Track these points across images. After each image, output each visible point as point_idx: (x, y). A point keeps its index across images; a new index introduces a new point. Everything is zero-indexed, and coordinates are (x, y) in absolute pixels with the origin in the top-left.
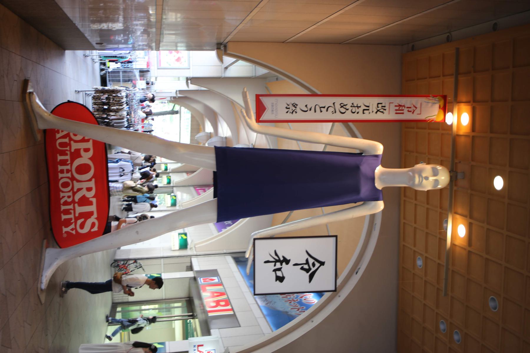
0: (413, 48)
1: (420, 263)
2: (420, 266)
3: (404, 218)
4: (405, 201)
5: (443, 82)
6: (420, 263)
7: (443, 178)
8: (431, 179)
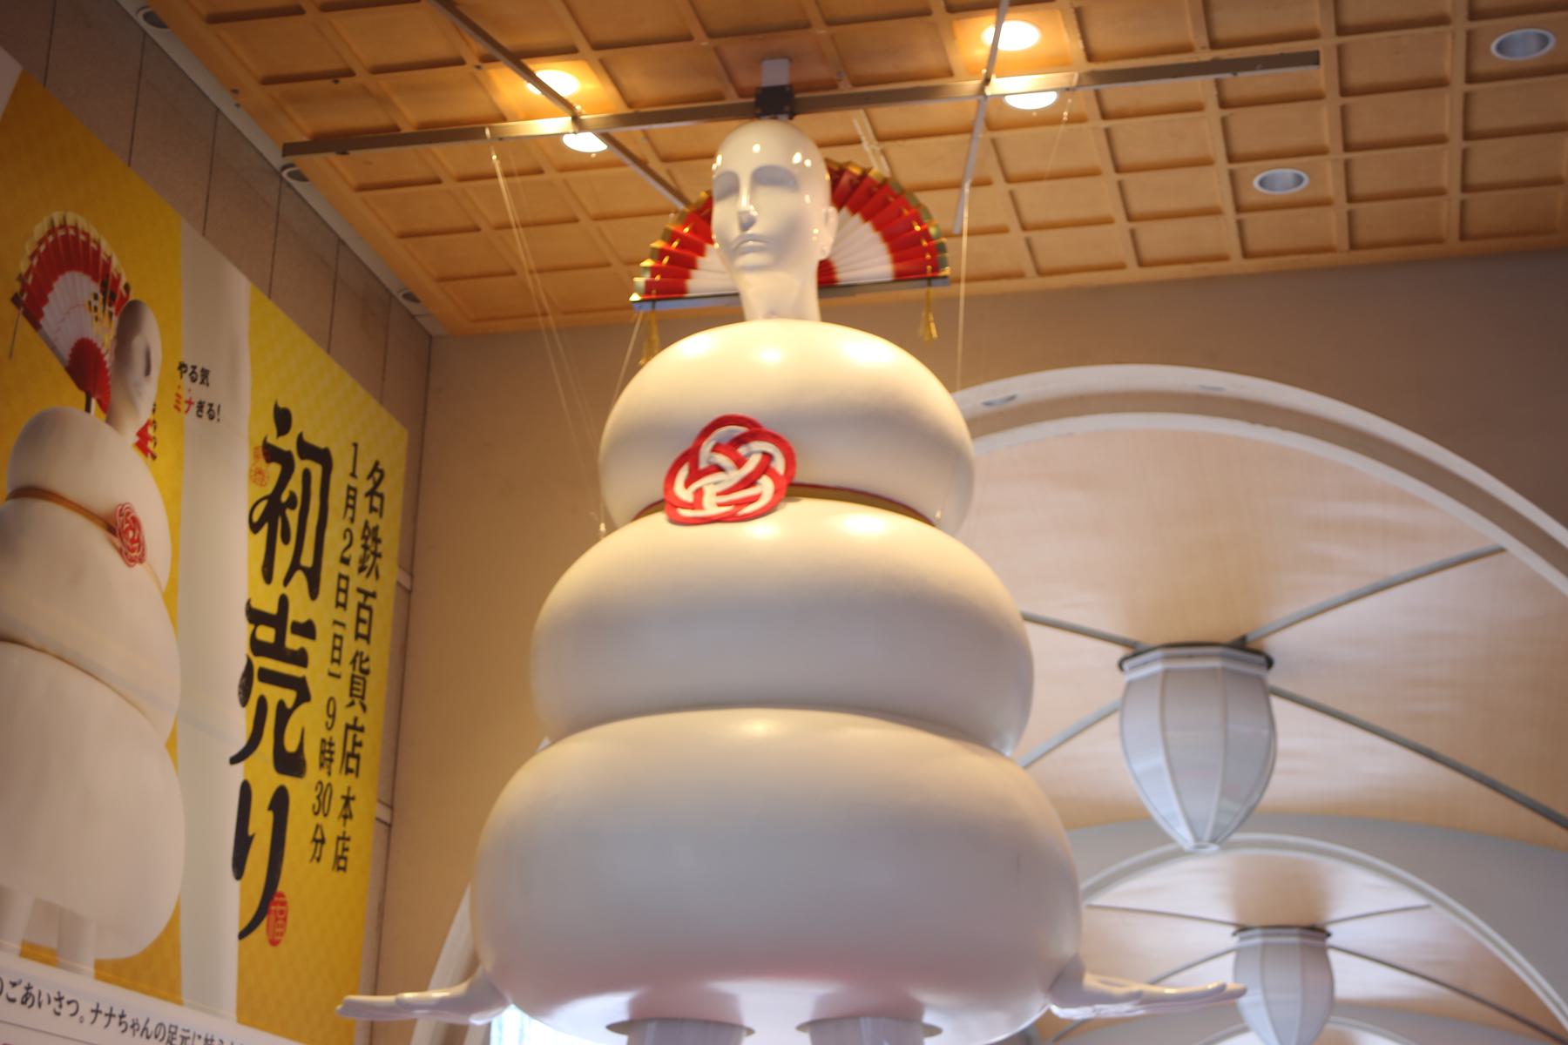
0: (410, 297)
1: (1283, 178)
2: (1299, 180)
3: (1121, 266)
4: (1040, 272)
5: (462, 179)
6: (1283, 178)
7: (750, 147)
8: (744, 201)
